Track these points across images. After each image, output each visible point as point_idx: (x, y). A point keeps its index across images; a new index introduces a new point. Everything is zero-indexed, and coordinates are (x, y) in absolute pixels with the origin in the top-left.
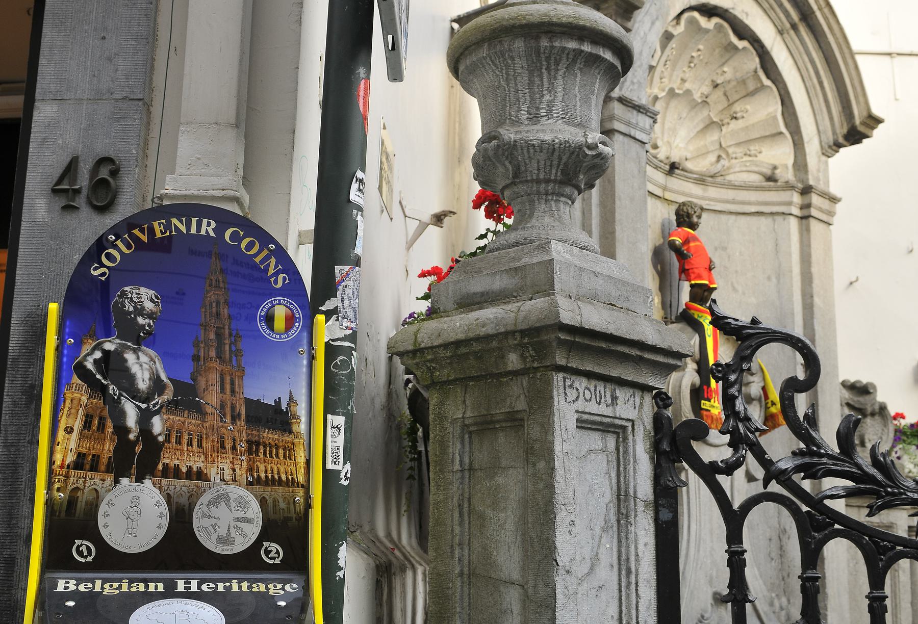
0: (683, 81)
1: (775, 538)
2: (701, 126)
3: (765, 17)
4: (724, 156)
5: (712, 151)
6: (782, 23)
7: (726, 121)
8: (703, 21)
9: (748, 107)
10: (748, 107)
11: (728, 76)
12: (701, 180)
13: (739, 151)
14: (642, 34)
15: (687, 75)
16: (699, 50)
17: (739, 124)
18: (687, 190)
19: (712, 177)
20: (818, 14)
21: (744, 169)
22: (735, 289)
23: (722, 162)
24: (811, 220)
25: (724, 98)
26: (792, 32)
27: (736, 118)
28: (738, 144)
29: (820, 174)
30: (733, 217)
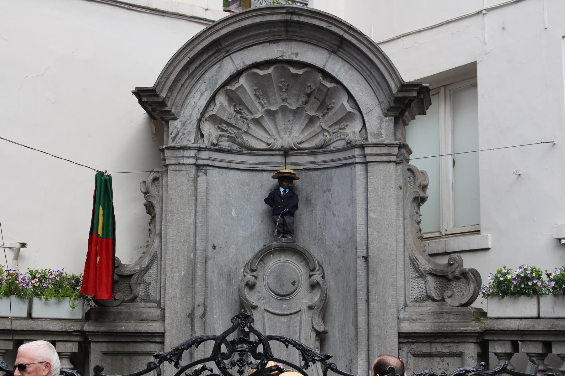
0: (284, 100)
1: (348, 365)
2: (306, 121)
3: (317, 48)
4: (326, 134)
6: (331, 47)
7: (325, 112)
8: (261, 73)
9: (334, 101)
10: (334, 101)
11: (313, 87)
12: (311, 152)
13: (335, 128)
14: (193, 103)
16: (281, 82)
17: (333, 111)
20: (346, 36)
21: (338, 138)
22: (334, 215)
23: (324, 138)
24: (369, 164)
25: (316, 100)
26: (341, 50)
28: (335, 124)
29: (383, 131)
30: (334, 170)
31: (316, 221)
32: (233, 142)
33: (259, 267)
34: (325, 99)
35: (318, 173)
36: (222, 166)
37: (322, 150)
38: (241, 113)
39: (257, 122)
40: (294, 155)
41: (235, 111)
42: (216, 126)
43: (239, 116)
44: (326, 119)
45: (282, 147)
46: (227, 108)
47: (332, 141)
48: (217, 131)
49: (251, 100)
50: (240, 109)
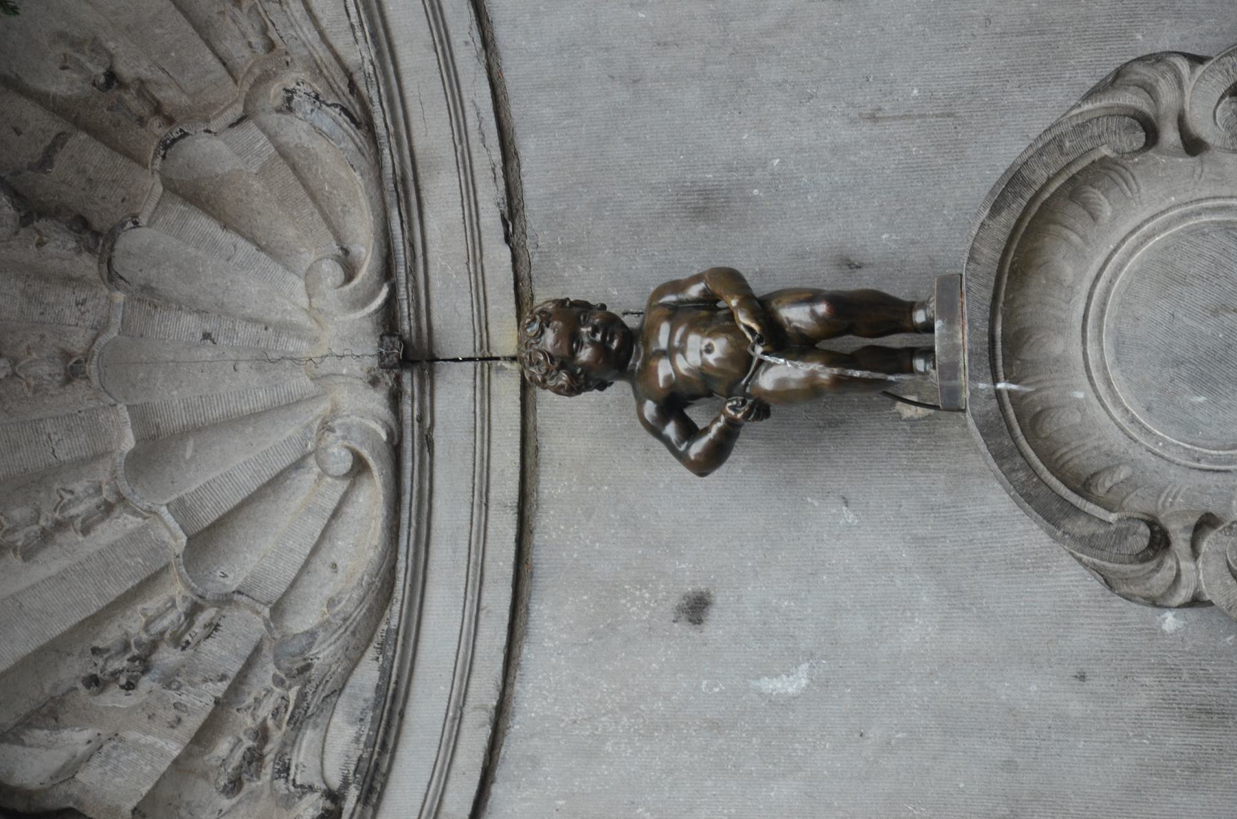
2: (202, 224)
4: (275, 92)
5: (272, 138)
15: (45, 369)
18: (459, 246)
19: (378, 152)
25: (61, 160)
27: (112, 77)
30: (502, 33)
31: (834, 150)
32: (338, 692)
33: (1137, 504)
34: (42, 99)
35: (528, 147)
36: (478, 760)
37: (378, 121)
38: (154, 646)
39: (206, 540)
40: (421, 307)
41: (130, 686)
42: (226, 803)
43: (168, 656)
44: (184, 100)
45: (374, 382)
46: (105, 732)
47: (321, 53)
48: (254, 796)
49: (62, 577)
50: (126, 647)
